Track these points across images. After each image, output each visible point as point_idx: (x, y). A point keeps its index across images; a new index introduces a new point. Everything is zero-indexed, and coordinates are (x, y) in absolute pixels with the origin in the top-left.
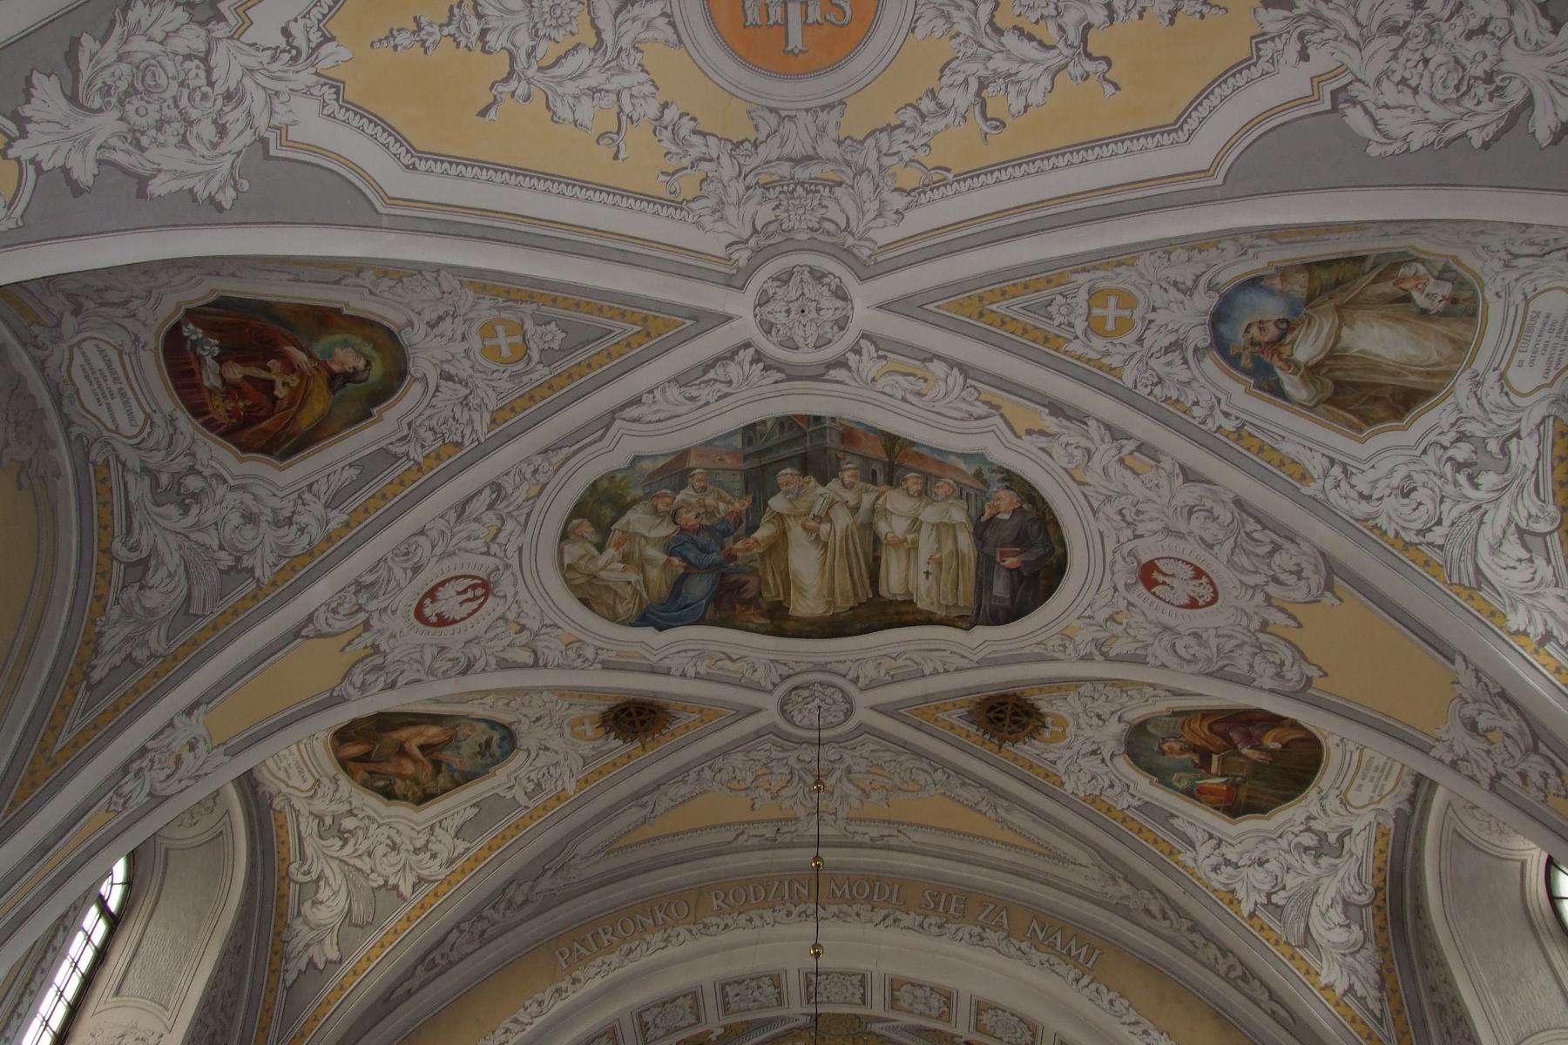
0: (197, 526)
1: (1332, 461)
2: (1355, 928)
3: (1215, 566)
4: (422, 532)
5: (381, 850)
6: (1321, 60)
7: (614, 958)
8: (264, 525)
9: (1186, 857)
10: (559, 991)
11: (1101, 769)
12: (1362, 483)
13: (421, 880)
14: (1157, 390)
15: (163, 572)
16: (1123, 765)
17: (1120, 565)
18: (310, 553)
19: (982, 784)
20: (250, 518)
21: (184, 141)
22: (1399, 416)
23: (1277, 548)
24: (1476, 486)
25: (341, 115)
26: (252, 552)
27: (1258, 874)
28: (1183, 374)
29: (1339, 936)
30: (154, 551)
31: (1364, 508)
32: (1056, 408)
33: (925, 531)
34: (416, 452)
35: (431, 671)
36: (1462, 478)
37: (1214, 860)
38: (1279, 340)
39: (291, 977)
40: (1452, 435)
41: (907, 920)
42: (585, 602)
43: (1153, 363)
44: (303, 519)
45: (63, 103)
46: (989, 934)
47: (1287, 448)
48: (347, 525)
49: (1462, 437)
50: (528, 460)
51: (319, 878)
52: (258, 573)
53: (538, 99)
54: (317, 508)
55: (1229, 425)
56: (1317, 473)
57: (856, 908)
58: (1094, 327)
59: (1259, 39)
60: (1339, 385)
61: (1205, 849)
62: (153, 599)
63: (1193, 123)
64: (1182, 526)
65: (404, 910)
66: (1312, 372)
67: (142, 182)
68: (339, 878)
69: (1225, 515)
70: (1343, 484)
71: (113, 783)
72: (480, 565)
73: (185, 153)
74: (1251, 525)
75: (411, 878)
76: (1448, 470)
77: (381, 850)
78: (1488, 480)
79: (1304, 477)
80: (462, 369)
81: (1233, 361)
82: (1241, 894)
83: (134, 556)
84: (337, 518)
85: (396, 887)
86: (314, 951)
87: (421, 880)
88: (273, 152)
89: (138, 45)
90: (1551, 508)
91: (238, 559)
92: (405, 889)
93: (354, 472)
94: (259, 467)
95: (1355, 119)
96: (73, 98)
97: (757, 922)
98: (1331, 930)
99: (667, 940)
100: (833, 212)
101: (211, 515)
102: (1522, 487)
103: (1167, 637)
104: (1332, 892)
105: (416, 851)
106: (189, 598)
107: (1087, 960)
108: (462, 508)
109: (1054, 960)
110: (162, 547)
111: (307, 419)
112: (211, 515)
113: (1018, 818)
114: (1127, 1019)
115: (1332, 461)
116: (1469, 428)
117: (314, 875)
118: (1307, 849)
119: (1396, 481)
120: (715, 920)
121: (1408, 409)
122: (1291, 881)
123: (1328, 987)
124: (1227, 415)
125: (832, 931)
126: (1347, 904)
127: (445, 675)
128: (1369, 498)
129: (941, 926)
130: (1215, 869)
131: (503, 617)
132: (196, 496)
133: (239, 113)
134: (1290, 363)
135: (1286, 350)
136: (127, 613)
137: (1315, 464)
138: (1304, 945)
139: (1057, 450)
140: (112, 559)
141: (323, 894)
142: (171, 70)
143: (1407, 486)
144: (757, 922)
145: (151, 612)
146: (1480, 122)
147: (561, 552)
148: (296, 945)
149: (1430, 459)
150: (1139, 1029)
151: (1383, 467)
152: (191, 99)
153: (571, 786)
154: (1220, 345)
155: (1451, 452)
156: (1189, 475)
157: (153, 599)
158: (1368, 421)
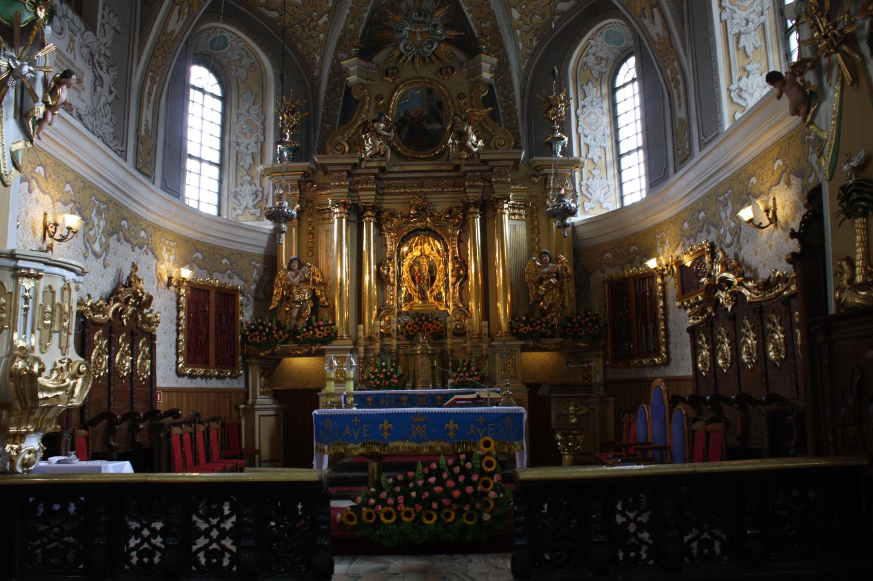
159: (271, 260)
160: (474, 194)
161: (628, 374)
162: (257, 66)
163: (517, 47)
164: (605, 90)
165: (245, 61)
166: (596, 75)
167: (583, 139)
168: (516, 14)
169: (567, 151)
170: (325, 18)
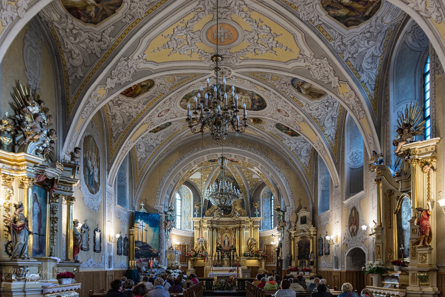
0: (122, 109)
1: (307, 104)
2: (308, 153)
3: (289, 113)
4: (159, 107)
5: (149, 140)
6: (307, 63)
7: (190, 153)
8: (133, 108)
9: (284, 142)
10: (181, 159)
11: (271, 128)
12: (311, 108)
13: (157, 145)
14: (282, 89)
15: (118, 117)
16: (275, 128)
17: (275, 108)
18: (141, 113)
19: (251, 128)
20: (130, 107)
21: (125, 76)
22: (319, 98)
23: (297, 114)
24: (328, 109)
25: (147, 63)
26: (132, 113)
27: (295, 145)
29: (305, 155)
30: (115, 113)
31: (311, 112)
32: (265, 88)
33: (243, 99)
35: (160, 122)
36: (326, 108)
37: (288, 142)
38: (302, 85)
39: (139, 160)
40: (326, 101)
41: (238, 146)
42: (184, 109)
43: (281, 85)
44: (139, 107)
45: (110, 80)
46: (252, 149)
48: (147, 108)
49: (327, 102)
50: (175, 94)
51: (140, 144)
52: (134, 116)
53: (178, 52)
54: (141, 105)
55: (292, 96)
56: (304, 105)
57: (230, 144)
59: (299, 58)
60: (310, 92)
61: (287, 141)
62: (118, 122)
63: (288, 63)
64: (284, 107)
66: (307, 90)
68: (143, 144)
69: (290, 108)
70: (308, 108)
72: (167, 108)
73: (126, 77)
74: (294, 110)
75: (155, 144)
76: (324, 106)
77: (149, 140)
78: (330, 109)
81: (294, 87)
82: (291, 148)
83: (112, 114)
84: (145, 107)
85: (153, 145)
86: (141, 156)
87: (157, 145)
88: (137, 71)
89: (119, 68)
90: (338, 114)
91: (130, 114)
92: (155, 146)
93: (146, 99)
97: (213, 146)
98: (304, 153)
99: (198, 150)
100: (228, 61)
101: (124, 107)
102: (334, 110)
103: (281, 118)
104: (306, 148)
105: (155, 140)
106: (123, 121)
107: (267, 154)
108: (164, 103)
109: (262, 154)
110: (117, 113)
113: (257, 133)
114: (272, 164)
115: (307, 104)
116: (329, 100)
117: (139, 144)
118: (303, 142)
119: (316, 108)
120: (206, 146)
121: (320, 97)
122: (300, 146)
123: (302, 162)
124: (292, 95)
126: (307, 150)
127: (162, 122)
128: (311, 110)
129: (244, 147)
130: (288, 144)
131: (171, 113)
133: (132, 69)
134: (303, 88)
135: (303, 86)
137: (304, 104)
138: (299, 156)
139: (265, 93)
140: (109, 115)
141: (141, 147)
142: (123, 68)
143: (318, 108)
144: (213, 146)
145: (118, 124)
147: (180, 103)
149: (322, 105)
150: (273, 165)
151: (314, 105)
152: (126, 71)
153: (181, 129)
154: (293, 84)
155: (325, 104)
156: (285, 102)
158: (314, 98)
162: (189, 192)
163: (249, 189)
164: (269, 199)
165: (186, 191)
166: (267, 196)
167: (263, 212)
168: (249, 182)
170: (205, 182)
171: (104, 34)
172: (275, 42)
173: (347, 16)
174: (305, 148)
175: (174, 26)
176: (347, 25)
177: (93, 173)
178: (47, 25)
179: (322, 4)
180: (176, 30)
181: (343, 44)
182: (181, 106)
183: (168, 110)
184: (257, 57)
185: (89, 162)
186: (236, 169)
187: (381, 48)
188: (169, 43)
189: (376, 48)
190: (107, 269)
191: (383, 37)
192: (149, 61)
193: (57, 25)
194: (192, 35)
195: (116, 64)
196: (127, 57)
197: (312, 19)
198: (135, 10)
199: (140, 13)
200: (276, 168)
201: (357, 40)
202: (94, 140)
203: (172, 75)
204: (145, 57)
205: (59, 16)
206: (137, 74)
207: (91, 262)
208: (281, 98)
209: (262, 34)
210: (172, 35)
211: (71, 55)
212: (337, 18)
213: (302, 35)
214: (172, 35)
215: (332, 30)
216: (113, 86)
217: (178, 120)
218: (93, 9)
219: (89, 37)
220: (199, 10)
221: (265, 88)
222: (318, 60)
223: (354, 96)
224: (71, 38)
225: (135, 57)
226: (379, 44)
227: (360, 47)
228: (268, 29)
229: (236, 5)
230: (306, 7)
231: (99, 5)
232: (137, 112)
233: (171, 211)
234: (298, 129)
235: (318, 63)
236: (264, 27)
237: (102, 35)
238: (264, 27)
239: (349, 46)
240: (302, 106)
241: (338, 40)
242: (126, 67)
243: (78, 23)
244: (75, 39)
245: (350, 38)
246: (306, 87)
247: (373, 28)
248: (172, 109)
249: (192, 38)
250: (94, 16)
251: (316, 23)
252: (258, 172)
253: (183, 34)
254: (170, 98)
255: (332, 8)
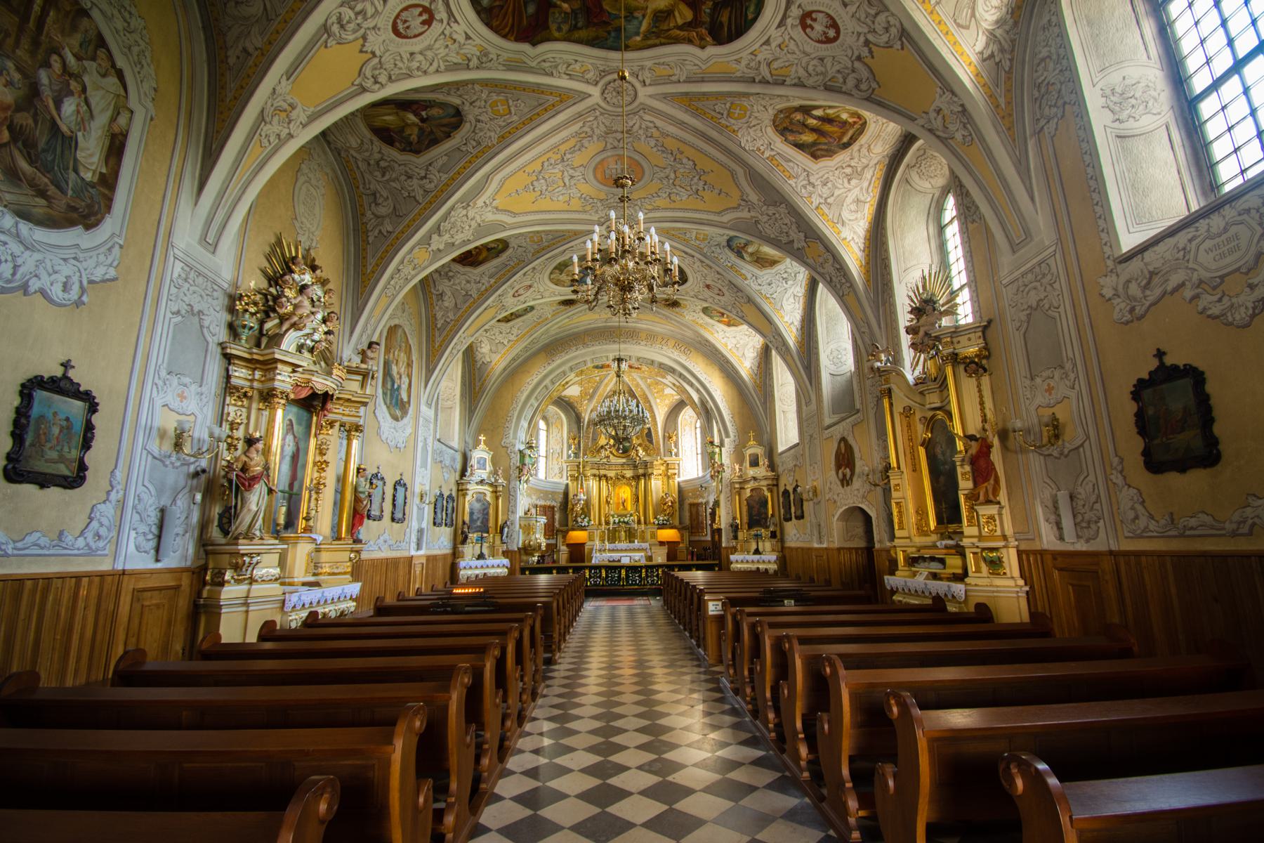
3: (725, 290)
6: (753, 214)
12: (759, 281)
13: (509, 341)
18: (486, 290)
20: (468, 282)
28: (718, 250)
30: (443, 292)
32: (686, 253)
34: (512, 263)
41: (642, 343)
47: (743, 271)
58: (696, 238)
59: (740, 205)
62: (446, 304)
65: (506, 348)
66: (752, 254)
67: (453, 244)
71: (451, 352)
72: (529, 283)
78: (790, 283)
79: (746, 279)
80: (524, 245)
81: (733, 250)
84: (492, 281)
92: (506, 343)
94: (468, 269)
95: (759, 226)
96: (440, 235)
101: (457, 281)
108: (524, 274)
111: (481, 258)
112: (457, 281)
122: (741, 342)
125: (623, 346)
132: (452, 277)
134: (746, 252)
136: (441, 308)
137: (749, 276)
146: (784, 239)
148: (478, 358)
156: (718, 273)
157: (446, 304)
159: (566, 494)
160: (641, 471)
161: (697, 538)
162: (560, 418)
169: (677, 455)
171: (430, 168)
172: (701, 183)
173: (814, 144)
174: (751, 344)
175: (544, 158)
176: (815, 156)
177: (399, 387)
178: (339, 154)
179: (776, 127)
180: (546, 164)
181: (810, 183)
182: (551, 280)
183: (530, 286)
184: (673, 205)
185: (394, 368)
186: (639, 380)
187: (870, 190)
188: (535, 183)
189: (862, 189)
190: (413, 553)
191: (871, 173)
192: (501, 210)
193: (355, 154)
194: (571, 171)
195: (448, 213)
196: (467, 202)
197: (762, 148)
198: (481, 134)
199: (490, 137)
200: (705, 376)
201: (831, 178)
202: (405, 333)
203: (538, 232)
204: (495, 204)
205: (359, 142)
206: (481, 230)
207: (385, 542)
208: (711, 268)
209: (682, 170)
210: (540, 172)
211: (375, 198)
212: (800, 146)
213: (745, 172)
214: (540, 172)
215: (791, 164)
216: (441, 247)
217: (544, 303)
218: (416, 131)
219: (406, 172)
220: (583, 135)
221: (686, 253)
222: (771, 208)
223: (831, 261)
224: (378, 174)
225: (480, 202)
226: (865, 184)
227: (836, 188)
228: (691, 163)
229: (640, 128)
230: (750, 130)
231: (425, 125)
232: (478, 290)
233: (531, 447)
234: (740, 314)
235: (770, 213)
236: (685, 161)
237: (427, 170)
238: (685, 161)
239: (819, 187)
240: (746, 279)
241: (801, 178)
242: (465, 219)
243: (392, 153)
244: (383, 175)
245: (821, 174)
246: (750, 250)
247: (856, 160)
248: (535, 285)
249: (572, 177)
250: (416, 141)
251: (767, 154)
252: (674, 385)
253: (557, 171)
254: (534, 268)
255: (792, 131)
